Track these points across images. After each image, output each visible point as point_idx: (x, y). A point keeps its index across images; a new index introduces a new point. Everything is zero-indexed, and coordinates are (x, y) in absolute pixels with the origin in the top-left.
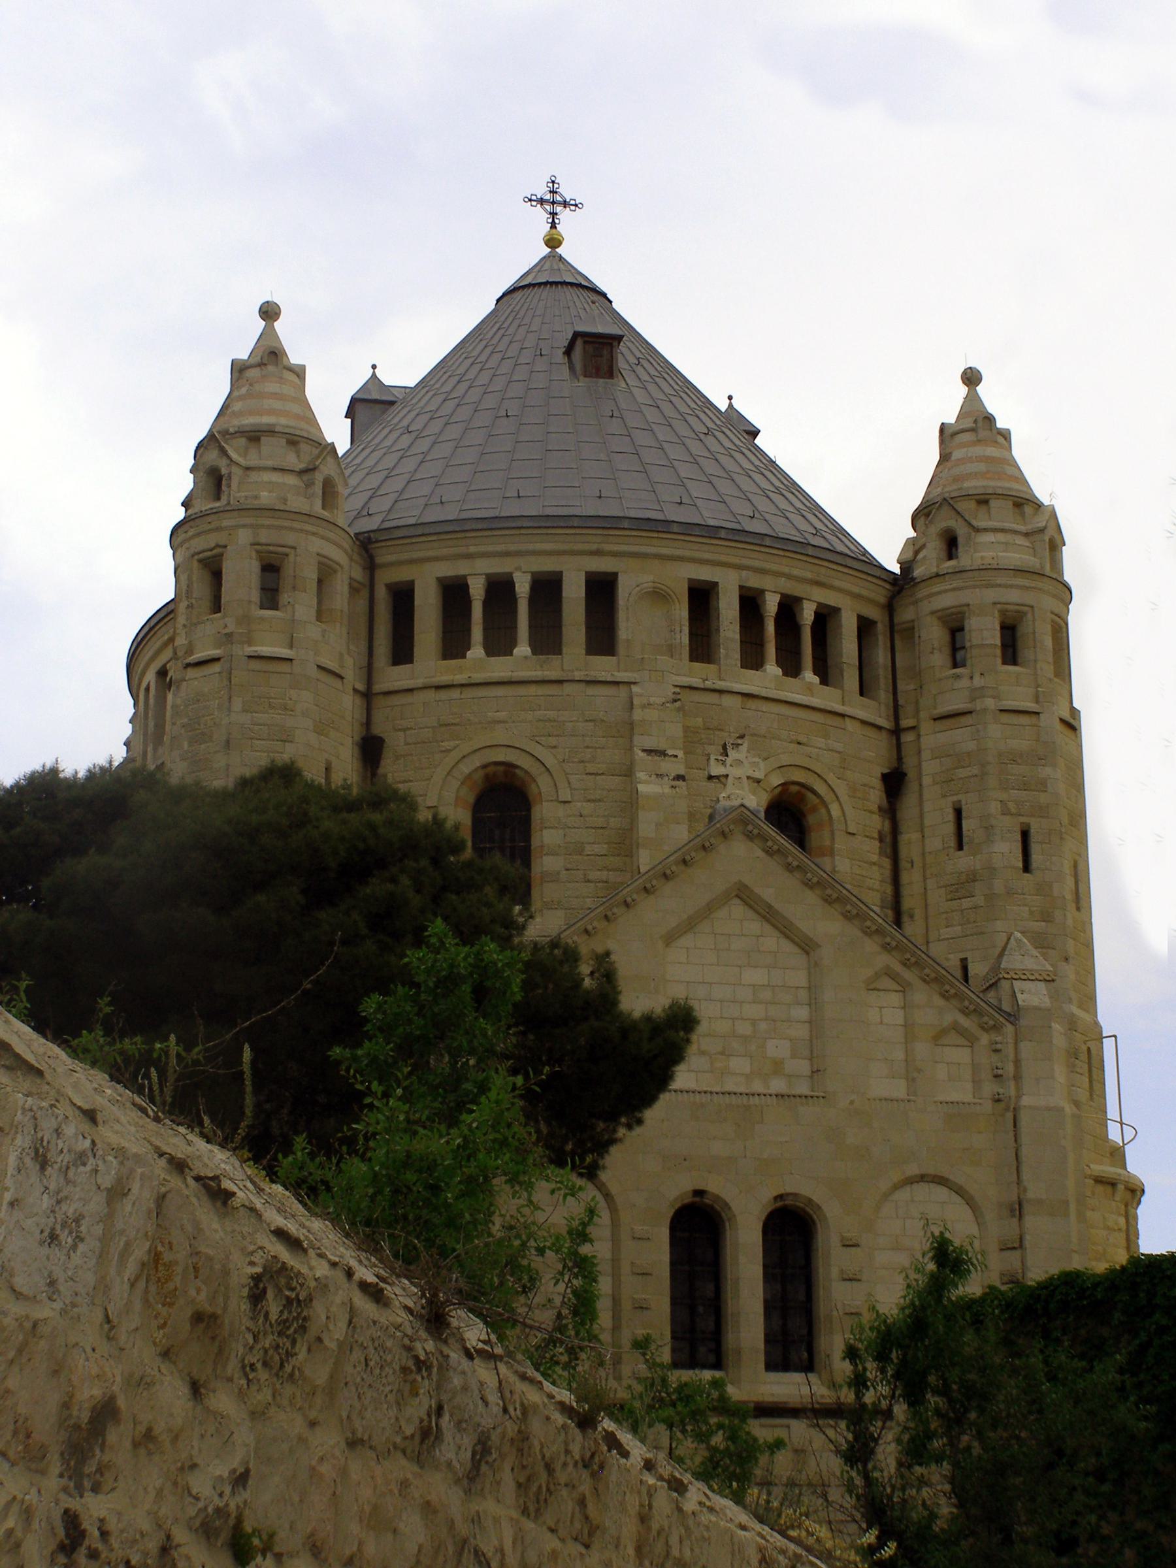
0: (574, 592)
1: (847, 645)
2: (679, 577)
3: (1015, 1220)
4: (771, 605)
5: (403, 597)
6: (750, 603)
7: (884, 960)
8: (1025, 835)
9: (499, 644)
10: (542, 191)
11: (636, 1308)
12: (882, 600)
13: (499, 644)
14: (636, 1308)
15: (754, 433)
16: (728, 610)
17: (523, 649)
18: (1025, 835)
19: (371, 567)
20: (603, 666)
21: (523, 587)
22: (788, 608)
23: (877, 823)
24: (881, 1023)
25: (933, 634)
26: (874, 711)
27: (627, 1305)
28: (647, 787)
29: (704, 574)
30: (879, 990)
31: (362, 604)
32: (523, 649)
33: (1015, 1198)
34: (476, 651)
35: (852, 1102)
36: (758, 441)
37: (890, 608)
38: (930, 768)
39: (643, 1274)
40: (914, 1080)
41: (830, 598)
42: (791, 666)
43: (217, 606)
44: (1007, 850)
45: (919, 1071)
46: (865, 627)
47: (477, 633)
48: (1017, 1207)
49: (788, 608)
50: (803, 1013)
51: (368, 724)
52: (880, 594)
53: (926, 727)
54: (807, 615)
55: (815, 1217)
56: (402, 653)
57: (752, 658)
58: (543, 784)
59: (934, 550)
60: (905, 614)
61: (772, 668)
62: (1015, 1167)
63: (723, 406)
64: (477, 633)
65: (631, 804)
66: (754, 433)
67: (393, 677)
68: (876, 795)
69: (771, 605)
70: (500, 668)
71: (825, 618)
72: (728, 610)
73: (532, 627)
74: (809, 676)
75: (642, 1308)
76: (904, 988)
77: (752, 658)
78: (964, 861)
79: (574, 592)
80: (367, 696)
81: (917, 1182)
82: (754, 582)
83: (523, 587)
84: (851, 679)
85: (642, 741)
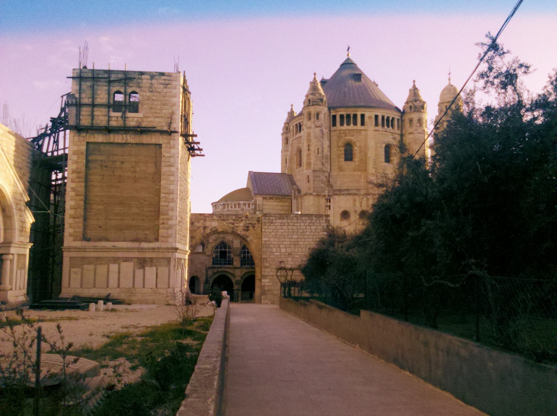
1: (396, 123)
2: (373, 115)
4: (386, 117)
5: (334, 117)
6: (383, 117)
9: (348, 124)
12: (400, 116)
13: (348, 124)
15: (377, 86)
16: (380, 118)
20: (363, 128)
21: (352, 116)
22: (388, 118)
26: (399, 132)
29: (377, 114)
31: (329, 117)
34: (345, 125)
36: (378, 87)
37: (401, 117)
41: (393, 116)
42: (388, 126)
46: (398, 120)
47: (345, 121)
49: (388, 118)
53: (407, 134)
54: (391, 119)
56: (334, 124)
60: (403, 118)
63: (373, 81)
64: (345, 121)
66: (377, 86)
71: (393, 119)
72: (380, 118)
73: (353, 122)
74: (391, 128)
77: (383, 126)
82: (384, 114)
83: (352, 116)
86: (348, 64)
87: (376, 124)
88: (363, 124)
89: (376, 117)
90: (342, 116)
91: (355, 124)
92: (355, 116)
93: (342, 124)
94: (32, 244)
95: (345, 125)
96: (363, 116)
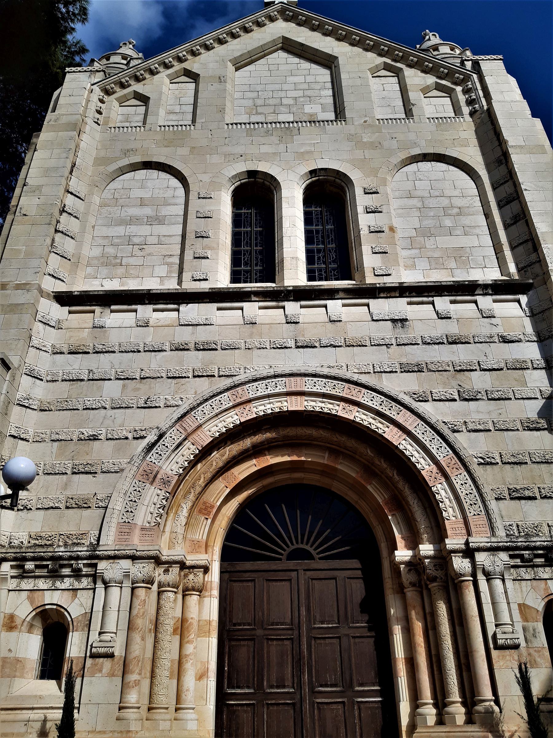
3: (503, 167)
7: (381, 60)
11: (198, 237)
14: (198, 237)
24: (384, 90)
27: (190, 235)
30: (379, 77)
33: (500, 153)
35: (365, 122)
39: (205, 217)
40: (411, 110)
45: (413, 105)
48: (502, 158)
50: (330, 92)
55: (343, 184)
62: (495, 139)
75: (203, 237)
76: (398, 73)
81: (422, 161)
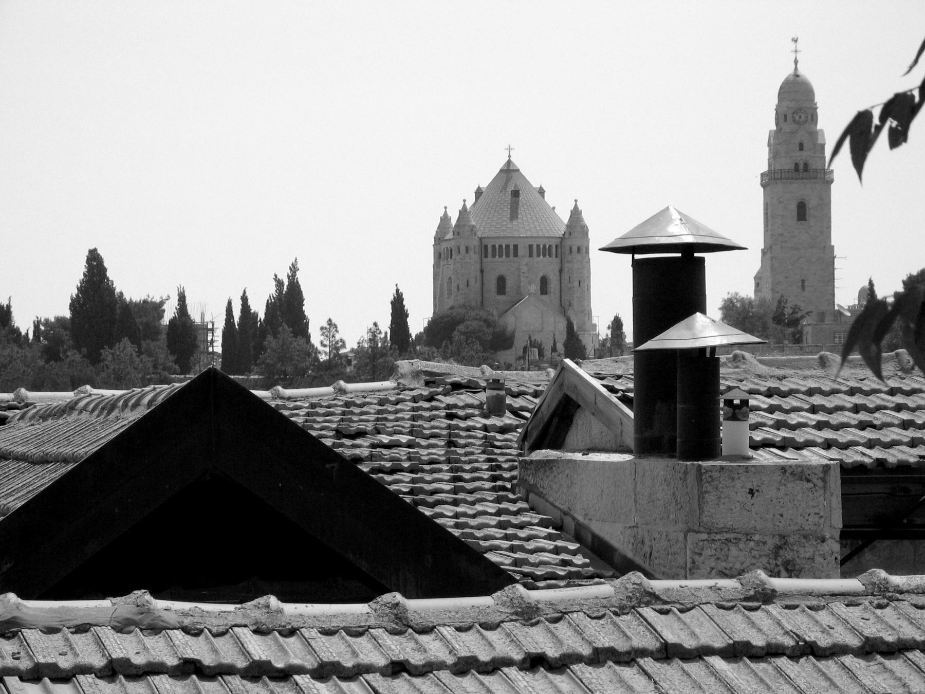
0: (511, 247)
5: (486, 247)
8: (580, 281)
9: (500, 256)
10: (511, 147)
13: (500, 256)
16: (535, 248)
17: (504, 257)
18: (580, 281)
19: (481, 243)
20: (516, 259)
21: (504, 247)
22: (544, 246)
23: (559, 278)
25: (567, 248)
26: (558, 260)
28: (522, 279)
32: (504, 257)
34: (497, 257)
38: (566, 270)
42: (544, 256)
43: (459, 252)
44: (576, 284)
46: (556, 246)
49: (544, 246)
51: (482, 266)
52: (560, 240)
54: (547, 247)
56: (486, 256)
57: (538, 256)
58: (507, 278)
59: (567, 234)
60: (563, 244)
61: (542, 257)
65: (520, 281)
67: (485, 260)
68: (558, 274)
69: (542, 246)
70: (501, 259)
72: (535, 248)
74: (547, 257)
78: (570, 285)
79: (511, 247)
80: (481, 263)
83: (504, 247)
84: (554, 256)
85: (522, 271)
86: (509, 172)
87: (531, 255)
88: (516, 255)
89: (531, 247)
90: (494, 246)
91: (508, 255)
92: (508, 246)
93: (494, 256)
94: (323, 358)
95: (497, 257)
96: (516, 247)
